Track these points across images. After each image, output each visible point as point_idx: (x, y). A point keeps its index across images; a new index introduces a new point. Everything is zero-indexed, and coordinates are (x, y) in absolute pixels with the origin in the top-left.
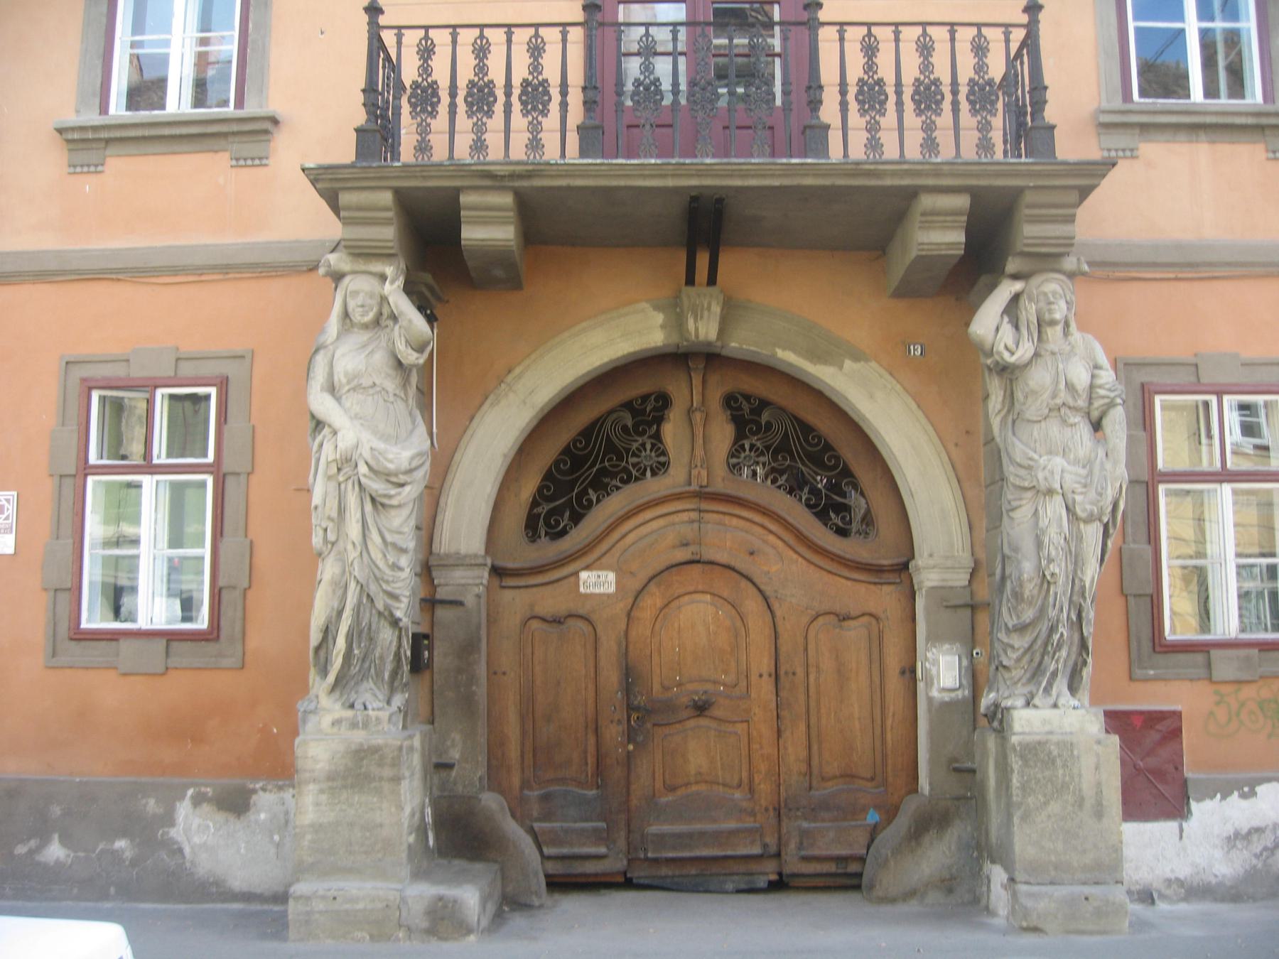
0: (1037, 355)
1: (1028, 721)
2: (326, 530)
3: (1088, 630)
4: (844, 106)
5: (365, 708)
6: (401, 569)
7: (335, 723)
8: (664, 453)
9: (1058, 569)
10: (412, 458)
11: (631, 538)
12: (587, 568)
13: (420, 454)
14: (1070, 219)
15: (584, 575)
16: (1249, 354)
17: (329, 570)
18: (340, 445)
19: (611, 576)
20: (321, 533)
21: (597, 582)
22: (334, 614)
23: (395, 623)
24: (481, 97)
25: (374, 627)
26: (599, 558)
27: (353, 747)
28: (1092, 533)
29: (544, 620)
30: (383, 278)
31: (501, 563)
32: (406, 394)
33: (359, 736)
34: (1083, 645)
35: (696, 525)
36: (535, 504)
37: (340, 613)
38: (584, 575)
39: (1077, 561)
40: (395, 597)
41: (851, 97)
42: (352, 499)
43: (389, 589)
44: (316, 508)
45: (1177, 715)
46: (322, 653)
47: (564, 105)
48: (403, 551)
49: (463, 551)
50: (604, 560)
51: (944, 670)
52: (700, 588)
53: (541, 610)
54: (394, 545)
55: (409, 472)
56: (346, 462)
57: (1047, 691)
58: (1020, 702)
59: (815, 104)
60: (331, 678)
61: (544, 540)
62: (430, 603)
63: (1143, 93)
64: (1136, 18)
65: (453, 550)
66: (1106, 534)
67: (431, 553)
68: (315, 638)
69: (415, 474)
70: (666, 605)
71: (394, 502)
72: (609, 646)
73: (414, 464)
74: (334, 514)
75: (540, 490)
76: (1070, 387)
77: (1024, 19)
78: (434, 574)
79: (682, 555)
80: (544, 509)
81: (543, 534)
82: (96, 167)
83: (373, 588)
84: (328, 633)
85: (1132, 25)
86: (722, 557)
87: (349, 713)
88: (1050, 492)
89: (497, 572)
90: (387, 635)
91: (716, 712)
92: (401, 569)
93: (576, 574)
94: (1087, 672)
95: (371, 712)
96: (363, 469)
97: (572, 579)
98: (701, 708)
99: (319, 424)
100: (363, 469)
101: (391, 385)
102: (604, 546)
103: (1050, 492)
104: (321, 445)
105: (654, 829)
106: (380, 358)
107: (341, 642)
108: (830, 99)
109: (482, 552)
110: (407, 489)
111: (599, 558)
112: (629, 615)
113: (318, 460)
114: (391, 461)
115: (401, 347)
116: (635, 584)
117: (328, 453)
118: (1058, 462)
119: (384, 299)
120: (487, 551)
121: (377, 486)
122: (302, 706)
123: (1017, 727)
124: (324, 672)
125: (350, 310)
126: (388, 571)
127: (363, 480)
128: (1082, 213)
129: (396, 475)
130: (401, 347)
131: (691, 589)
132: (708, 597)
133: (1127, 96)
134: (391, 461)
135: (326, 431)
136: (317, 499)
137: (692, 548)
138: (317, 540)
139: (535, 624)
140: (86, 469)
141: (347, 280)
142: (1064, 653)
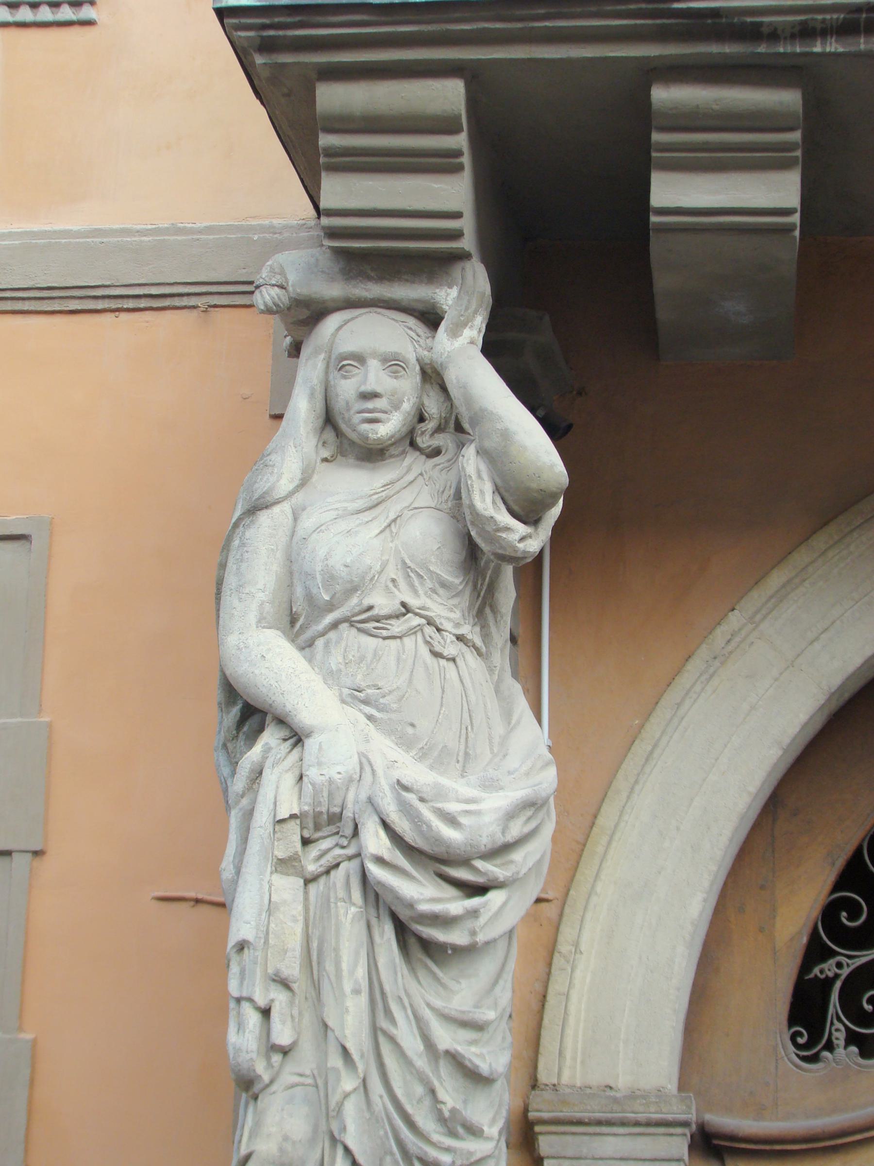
2: (266, 1013)
6: (474, 1131)
10: (511, 815)
13: (533, 805)
18: (313, 773)
20: (253, 1018)
30: (431, 318)
31: (725, 1121)
32: (486, 636)
36: (815, 952)
44: (241, 946)
48: (474, 1077)
49: (623, 1081)
54: (455, 1060)
56: (325, 822)
61: (845, 1055)
65: (596, 1078)
67: (534, 1085)
69: (517, 856)
71: (456, 937)
73: (516, 830)
74: (292, 968)
75: (830, 913)
78: (545, 1144)
80: (843, 964)
81: (840, 1037)
92: (474, 1131)
96: (375, 841)
99: (251, 715)
101: (450, 612)
104: (258, 773)
106: (425, 534)
109: (672, 1087)
110: (495, 898)
114: (451, 820)
115: (485, 502)
117: (280, 793)
119: (432, 376)
120: (682, 1086)
121: (420, 892)
125: (339, 405)
127: (376, 871)
129: (465, 862)
130: (485, 502)
134: (451, 820)
135: (270, 737)
136: (244, 924)
138: (243, 1039)
141: (332, 322)
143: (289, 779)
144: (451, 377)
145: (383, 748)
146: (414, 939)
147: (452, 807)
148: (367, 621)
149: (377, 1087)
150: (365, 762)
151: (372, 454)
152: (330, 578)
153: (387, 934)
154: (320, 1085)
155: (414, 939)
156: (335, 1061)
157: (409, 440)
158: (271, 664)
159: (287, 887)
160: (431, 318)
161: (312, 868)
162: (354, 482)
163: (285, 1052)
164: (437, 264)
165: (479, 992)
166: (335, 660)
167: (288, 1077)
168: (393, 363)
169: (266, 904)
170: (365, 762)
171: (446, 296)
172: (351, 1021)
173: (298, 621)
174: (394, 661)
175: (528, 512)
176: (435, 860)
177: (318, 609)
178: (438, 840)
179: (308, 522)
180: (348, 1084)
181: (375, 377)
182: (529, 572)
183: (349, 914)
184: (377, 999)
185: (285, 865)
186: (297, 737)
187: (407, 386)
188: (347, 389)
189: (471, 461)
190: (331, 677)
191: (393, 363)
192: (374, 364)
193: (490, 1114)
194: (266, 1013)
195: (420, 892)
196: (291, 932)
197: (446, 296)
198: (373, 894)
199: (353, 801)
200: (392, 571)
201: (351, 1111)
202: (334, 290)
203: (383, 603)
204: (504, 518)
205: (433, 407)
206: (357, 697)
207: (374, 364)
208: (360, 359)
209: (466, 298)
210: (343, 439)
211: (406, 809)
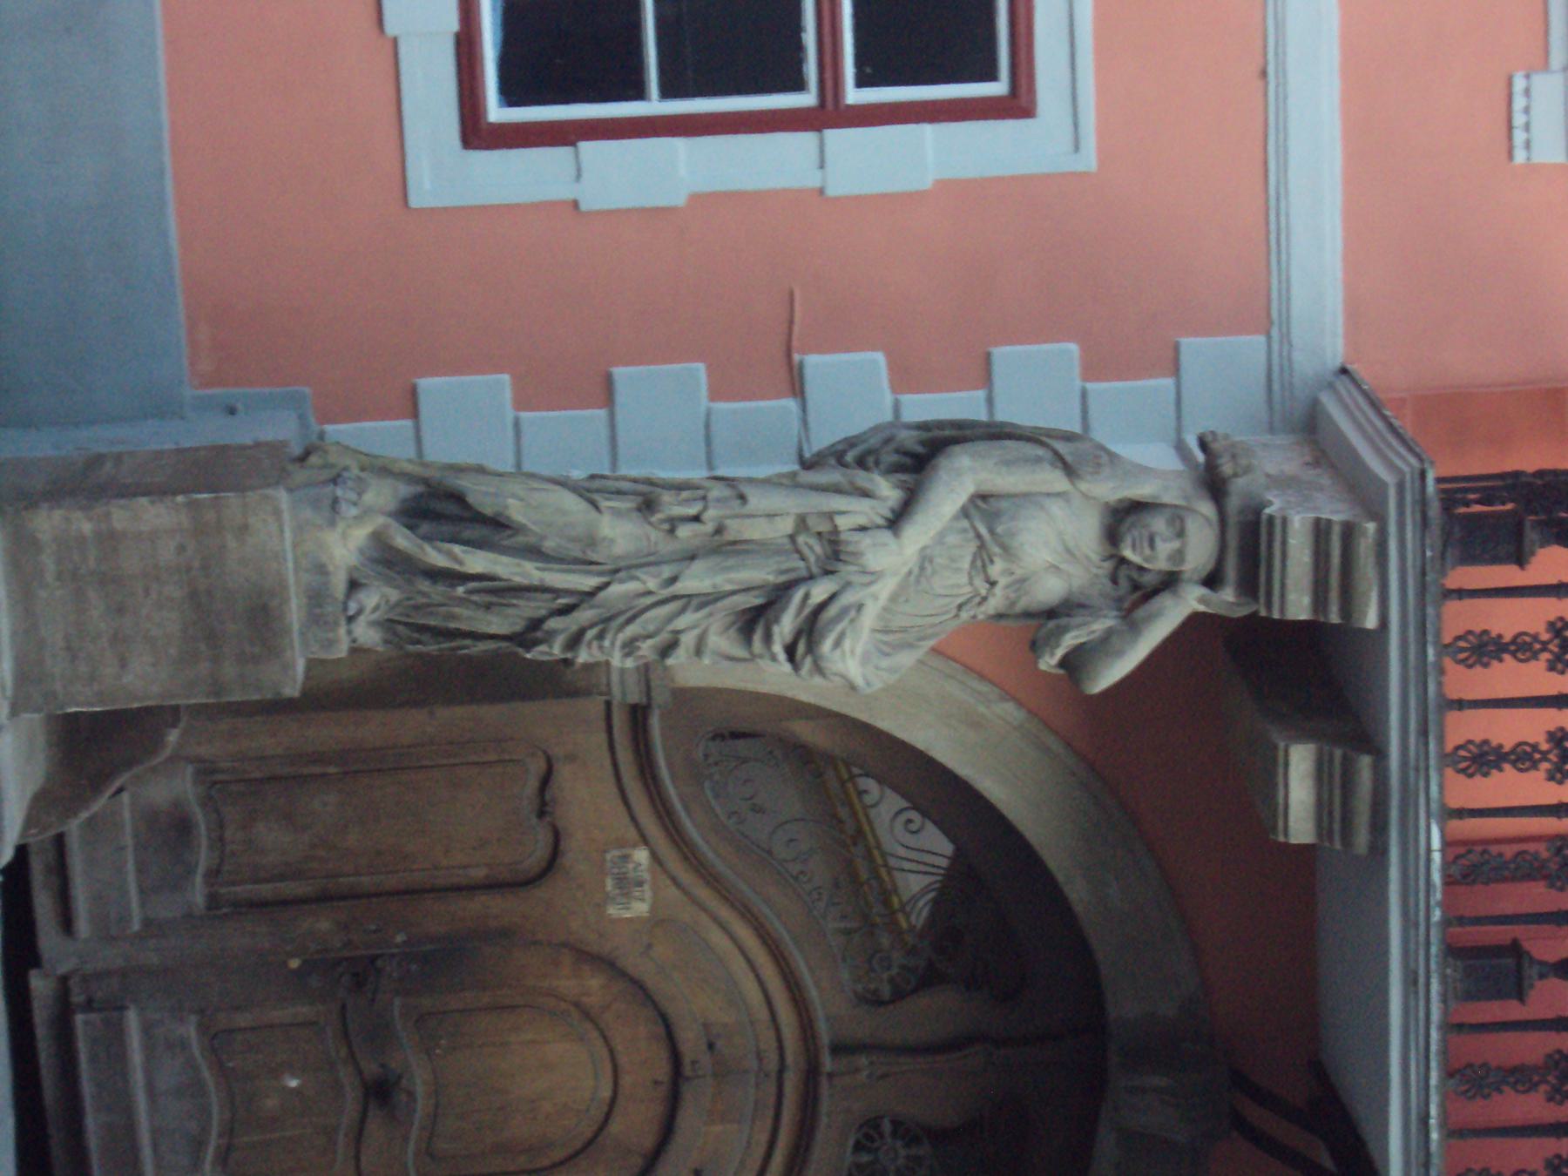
2: (696, 519)
5: (351, 619)
7: (321, 569)
8: (898, 996)
11: (717, 937)
12: (655, 857)
15: (641, 855)
18: (865, 541)
20: (692, 511)
22: (532, 540)
25: (510, 611)
26: (674, 880)
27: (274, 603)
29: (546, 781)
30: (1212, 581)
33: (295, 611)
35: (755, 1064)
37: (534, 552)
38: (641, 855)
42: (763, 573)
43: (590, 634)
46: (451, 508)
50: (673, 891)
52: (626, 1081)
53: (565, 774)
56: (835, 553)
60: (403, 540)
70: (586, 1015)
72: (498, 907)
79: (690, 1040)
83: (584, 616)
86: (688, 1118)
87: (339, 584)
89: (639, 715)
91: (376, 1129)
93: (645, 840)
95: (342, 631)
96: (820, 591)
97: (632, 833)
98: (381, 1092)
100: (820, 591)
102: (703, 893)
105: (132, 1019)
106: (1049, 590)
107: (476, 562)
110: (787, 667)
111: (674, 880)
112: (565, 945)
113: (837, 490)
114: (838, 643)
116: (632, 962)
117: (853, 512)
119: (1170, 582)
121: (786, 625)
126: (622, 637)
127: (798, 596)
131: (623, 1060)
132: (606, 1093)
137: (706, 1060)
139: (537, 767)
141: (1207, 508)
143: (862, 521)
144: (1165, 600)
145: (885, 588)
147: (847, 644)
148: (982, 557)
149: (649, 600)
150: (876, 576)
151: (1112, 536)
152: (1012, 535)
153: (755, 600)
154: (649, 561)
155: (753, 621)
156: (667, 571)
157: (1123, 561)
159: (786, 526)
160: (1212, 581)
161: (801, 539)
162: (1086, 531)
163: (672, 531)
164: (1249, 585)
166: (952, 539)
167: (654, 535)
168: (1179, 556)
170: (876, 576)
171: (1228, 594)
172: (696, 580)
173: (983, 503)
174: (955, 581)
176: (811, 629)
177: (992, 518)
178: (823, 637)
179: (1056, 508)
180: (652, 584)
181: (1165, 548)
184: (707, 600)
185: (802, 523)
186: (896, 521)
187: (1160, 562)
188: (1159, 524)
189: (1099, 626)
190: (940, 538)
191: (1179, 556)
192: (1176, 544)
194: (696, 519)
195: (786, 625)
196: (755, 531)
197: (1228, 594)
199: (847, 571)
200: (1019, 572)
201: (632, 586)
202: (1234, 503)
203: (996, 570)
204: (1060, 653)
205: (1147, 579)
206: (925, 559)
207: (1176, 544)
208: (1181, 534)
209: (1227, 599)
211: (845, 611)
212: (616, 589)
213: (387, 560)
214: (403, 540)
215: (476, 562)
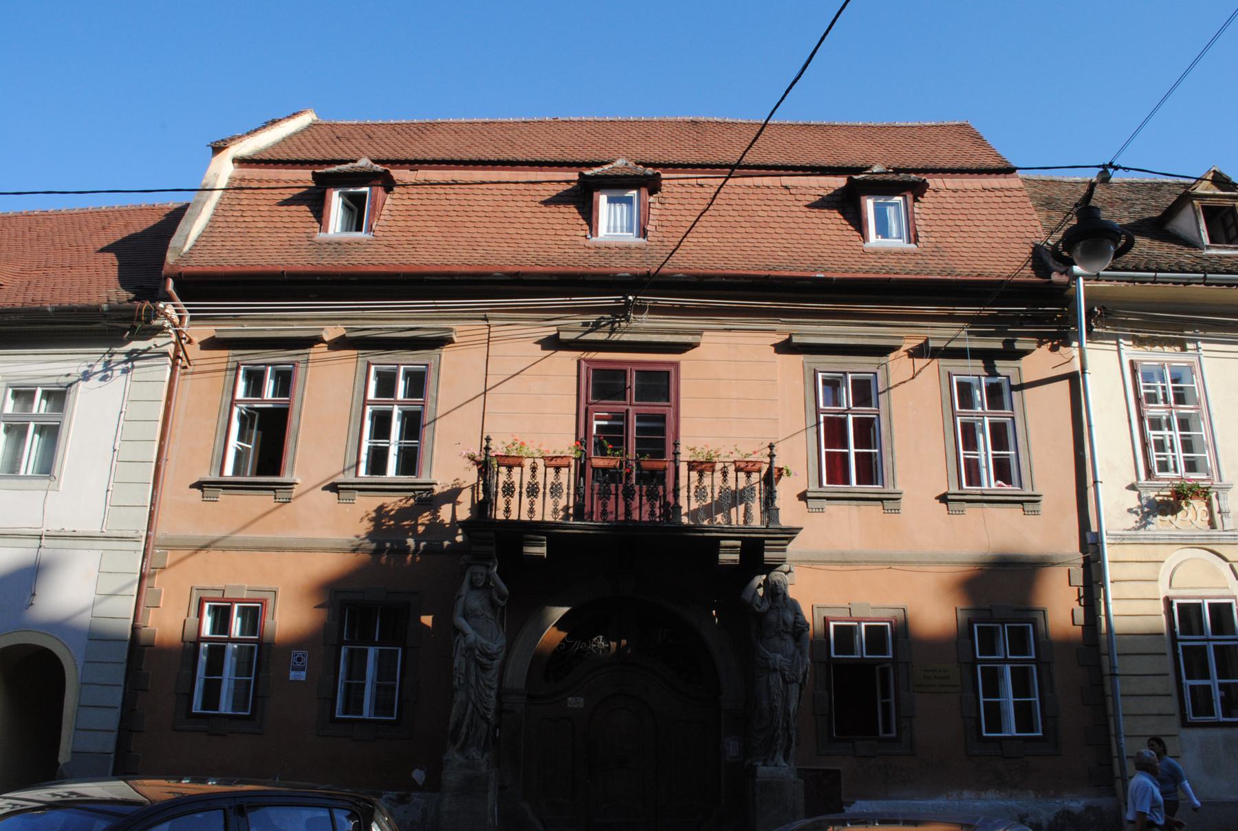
0: (771, 608)
1: (763, 771)
3: (793, 733)
4: (689, 497)
9: (779, 704)
14: (784, 550)
16: (873, 604)
17: (460, 697)
19: (582, 700)
21: (575, 702)
23: (487, 720)
24: (533, 491)
28: (794, 689)
34: (790, 740)
37: (465, 715)
39: (786, 701)
40: (488, 709)
41: (692, 494)
45: (838, 771)
47: (568, 494)
48: (491, 688)
51: (732, 748)
55: (497, 654)
56: (470, 649)
57: (773, 758)
58: (760, 763)
59: (676, 496)
60: (458, 746)
62: (499, 712)
63: (828, 482)
64: (826, 447)
66: (801, 689)
68: (451, 727)
76: (785, 623)
77: (768, 460)
82: (351, 501)
84: (458, 725)
85: (824, 450)
88: (775, 670)
90: (484, 726)
94: (793, 750)
96: (477, 652)
99: (458, 631)
100: (477, 652)
103: (775, 670)
107: (464, 730)
108: (683, 493)
115: (496, 598)
117: (462, 644)
118: (779, 656)
119: (488, 577)
121: (484, 660)
122: (445, 758)
123: (759, 774)
124: (455, 743)
128: (788, 548)
133: (820, 484)
136: (456, 665)
138: (456, 683)
140: (341, 643)
142: (780, 742)
145: (479, 637)
146: (484, 668)
151: (478, 588)
158: (461, 622)
160: (488, 567)
165: (492, 676)
169: (459, 661)
172: (473, 680)
173: (466, 616)
175: (502, 599)
182: (503, 608)
183: (473, 665)
184: (477, 678)
193: (493, 693)
195: (484, 660)
198: (477, 662)
206: (474, 629)
210: (473, 586)
212: (473, 697)
213: (462, 750)
214: (458, 746)
215: (464, 730)
